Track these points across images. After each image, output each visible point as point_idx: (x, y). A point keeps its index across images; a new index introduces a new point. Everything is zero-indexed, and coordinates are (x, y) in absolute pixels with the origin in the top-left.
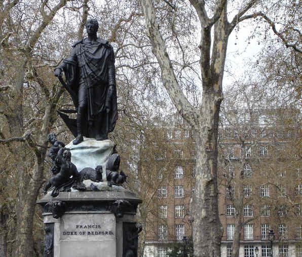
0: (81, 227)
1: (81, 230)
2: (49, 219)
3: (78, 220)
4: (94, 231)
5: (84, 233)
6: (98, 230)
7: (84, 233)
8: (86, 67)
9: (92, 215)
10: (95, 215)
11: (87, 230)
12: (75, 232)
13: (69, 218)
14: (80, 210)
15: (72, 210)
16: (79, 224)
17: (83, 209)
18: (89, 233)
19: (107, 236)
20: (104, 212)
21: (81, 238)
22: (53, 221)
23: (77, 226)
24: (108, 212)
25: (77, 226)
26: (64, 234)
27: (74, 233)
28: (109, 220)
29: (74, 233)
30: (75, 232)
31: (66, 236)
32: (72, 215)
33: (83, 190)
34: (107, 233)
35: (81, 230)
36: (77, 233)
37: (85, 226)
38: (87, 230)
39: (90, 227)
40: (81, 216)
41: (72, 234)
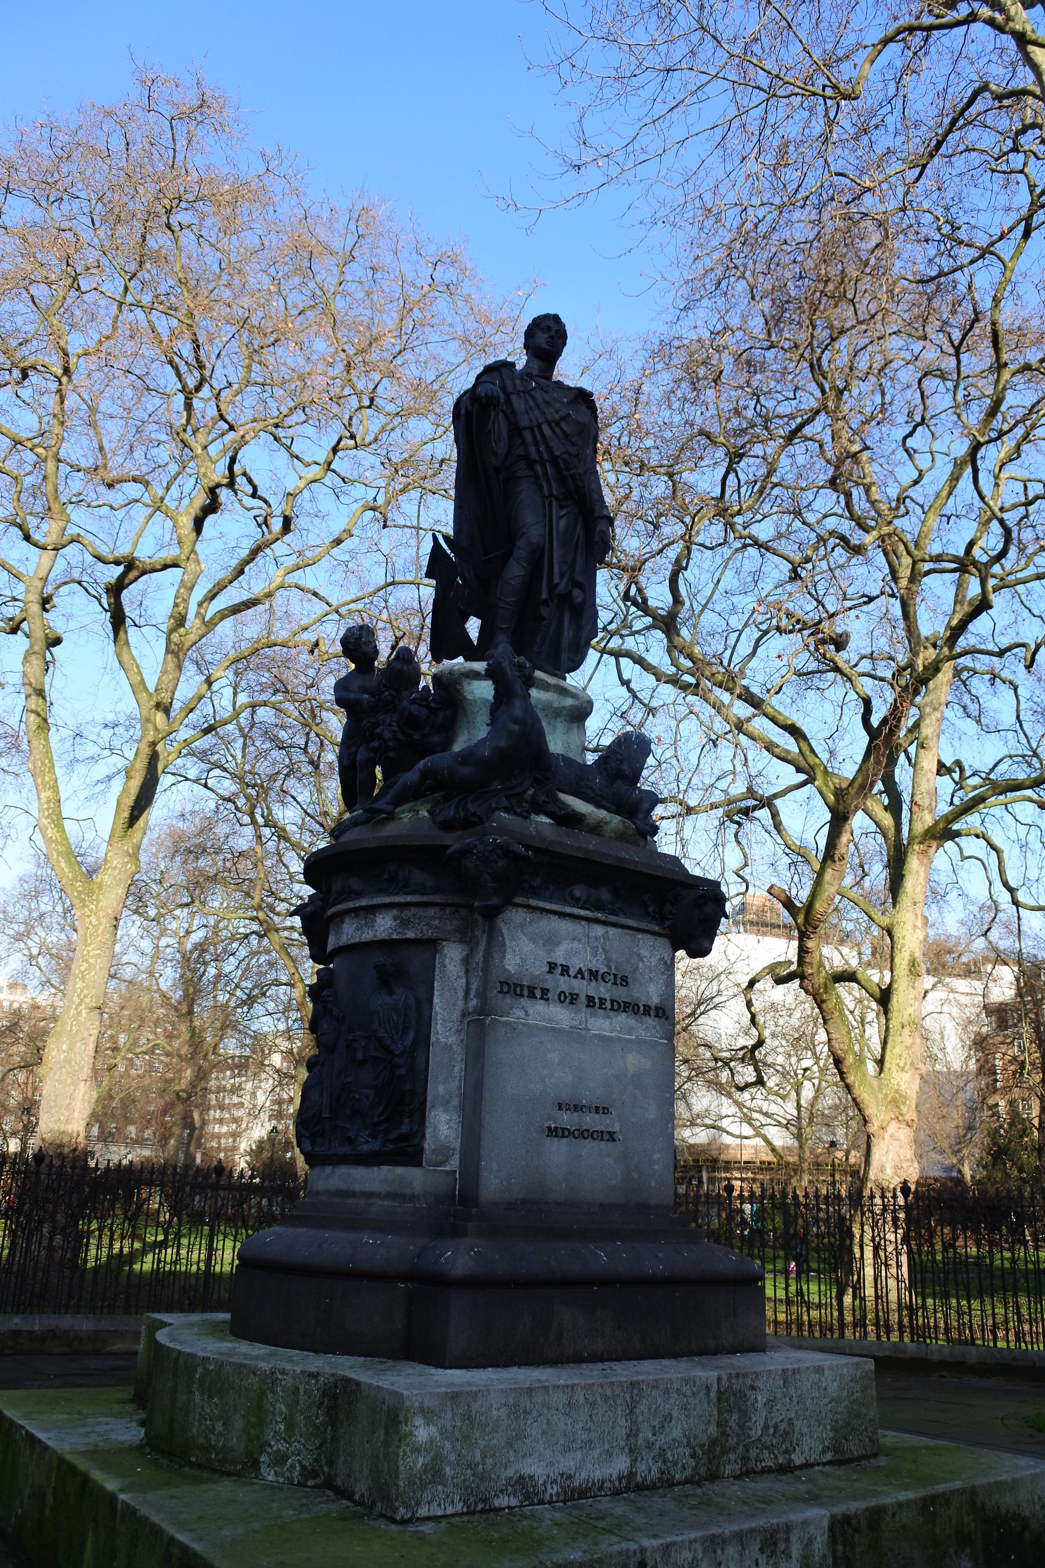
0: (565, 970)
1: (565, 984)
2: (405, 923)
3: (551, 941)
4: (607, 996)
5: (573, 998)
6: (621, 994)
7: (573, 998)
8: (545, 428)
9: (599, 930)
10: (612, 931)
11: (584, 988)
12: (545, 992)
13: (522, 926)
14: (564, 901)
15: (536, 893)
16: (559, 956)
17: (576, 902)
18: (590, 1000)
19: (650, 1021)
20: (643, 925)
21: (560, 1015)
22: (429, 934)
23: (552, 966)
24: (657, 928)
25: (552, 966)
26: (501, 992)
27: (538, 994)
28: (654, 961)
29: (538, 994)
30: (545, 992)
31: (508, 1000)
32: (537, 915)
33: (570, 820)
34: (647, 1010)
35: (565, 984)
36: (550, 996)
37: (580, 971)
38: (584, 988)
39: (594, 975)
40: (565, 926)
41: (532, 995)
